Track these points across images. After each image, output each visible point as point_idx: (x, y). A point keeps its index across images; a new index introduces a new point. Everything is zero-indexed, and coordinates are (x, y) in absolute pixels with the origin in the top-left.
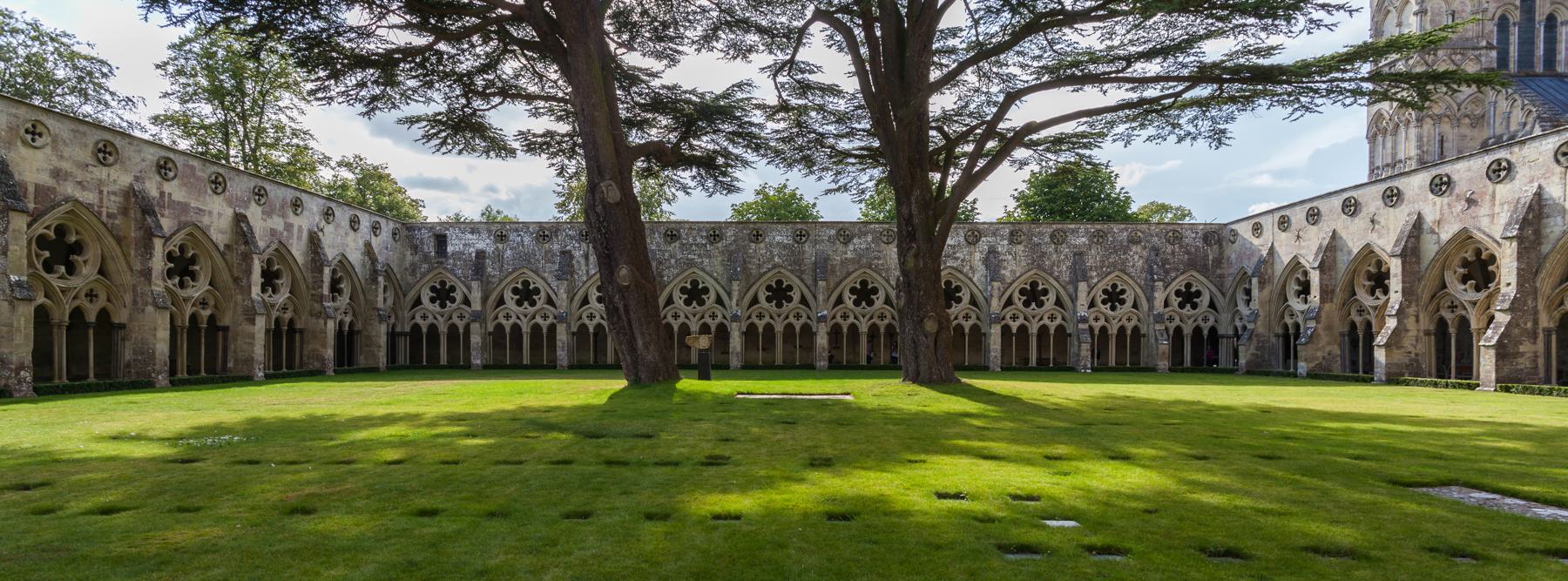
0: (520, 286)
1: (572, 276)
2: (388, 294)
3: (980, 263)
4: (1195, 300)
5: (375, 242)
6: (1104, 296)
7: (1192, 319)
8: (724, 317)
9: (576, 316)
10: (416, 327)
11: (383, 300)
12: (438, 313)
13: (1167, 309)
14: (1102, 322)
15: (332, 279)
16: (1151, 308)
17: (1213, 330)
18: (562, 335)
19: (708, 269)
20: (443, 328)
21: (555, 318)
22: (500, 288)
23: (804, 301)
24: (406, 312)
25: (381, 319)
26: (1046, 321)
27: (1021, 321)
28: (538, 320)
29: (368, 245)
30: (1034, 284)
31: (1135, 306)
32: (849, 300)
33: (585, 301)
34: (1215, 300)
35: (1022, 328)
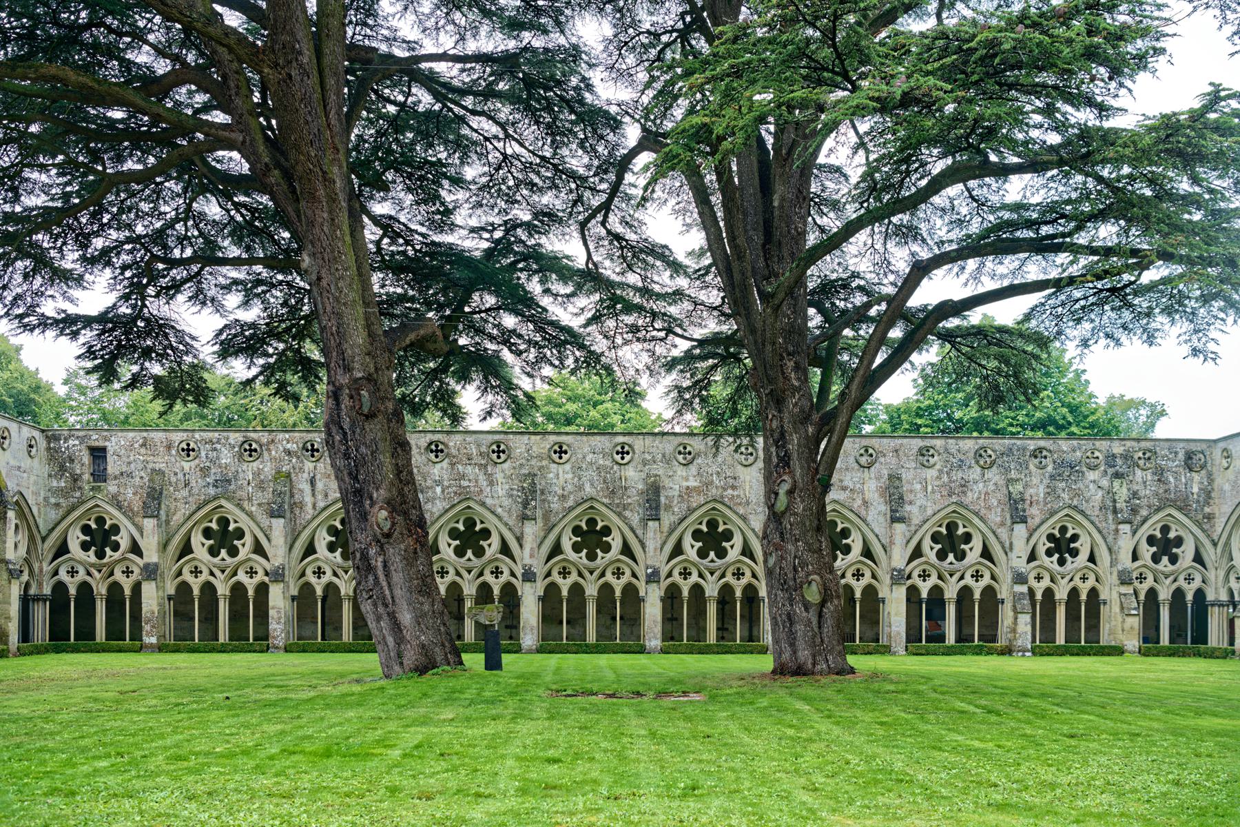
0: (214, 526)
2: (20, 536)
3: (876, 495)
4: (1174, 550)
6: (1049, 545)
7: (1172, 578)
8: (513, 574)
9: (297, 571)
10: (60, 587)
12: (93, 565)
13: (1137, 564)
14: (1046, 582)
17: (1200, 594)
19: (489, 501)
20: (101, 589)
21: (267, 574)
22: (184, 530)
23: (627, 550)
24: (45, 565)
25: (13, 574)
26: (968, 580)
27: (933, 580)
28: (242, 577)
30: (952, 527)
31: (1092, 559)
32: (691, 549)
33: (310, 550)
35: (936, 591)
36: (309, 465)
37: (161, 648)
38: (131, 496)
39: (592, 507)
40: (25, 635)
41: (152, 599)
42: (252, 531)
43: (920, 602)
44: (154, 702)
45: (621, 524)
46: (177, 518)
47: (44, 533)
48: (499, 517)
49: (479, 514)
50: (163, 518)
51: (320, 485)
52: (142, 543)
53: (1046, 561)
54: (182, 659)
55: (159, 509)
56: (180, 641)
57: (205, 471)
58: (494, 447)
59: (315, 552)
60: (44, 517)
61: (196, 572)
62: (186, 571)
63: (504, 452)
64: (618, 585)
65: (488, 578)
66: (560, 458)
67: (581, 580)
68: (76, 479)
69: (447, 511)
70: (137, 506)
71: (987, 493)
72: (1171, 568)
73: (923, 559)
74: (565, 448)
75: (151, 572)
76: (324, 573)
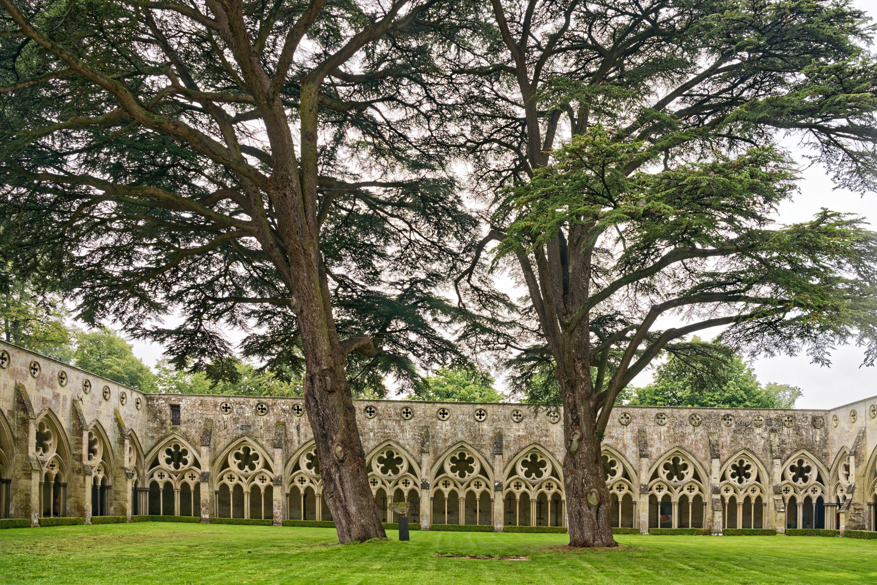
0: (241, 452)
8: (415, 484)
10: (154, 484)
11: (129, 460)
12: (172, 472)
13: (784, 482)
14: (731, 493)
15: (89, 441)
16: (771, 481)
17: (820, 499)
19: (401, 442)
20: (177, 486)
21: (272, 480)
23: (483, 471)
24: (146, 471)
25: (129, 476)
26: (686, 491)
27: (665, 491)
28: (257, 482)
30: (676, 460)
31: (758, 479)
32: (521, 471)
33: (297, 467)
34: (822, 474)
35: (667, 498)
36: (296, 419)
37: (211, 521)
38: (195, 433)
39: (462, 446)
40: (135, 511)
41: (206, 492)
43: (657, 504)
44: (208, 553)
45: (479, 456)
46: (220, 447)
47: (145, 453)
48: (407, 451)
49: (395, 449)
50: (212, 446)
51: (302, 430)
52: (200, 461)
53: (732, 480)
54: (223, 528)
55: (210, 441)
56: (221, 518)
57: (236, 420)
59: (299, 469)
60: (146, 444)
61: (231, 478)
62: (225, 477)
64: (478, 492)
65: (401, 486)
67: (456, 489)
68: (163, 423)
69: (376, 447)
70: (197, 439)
71: (696, 441)
72: (804, 484)
73: (659, 479)
75: (205, 477)
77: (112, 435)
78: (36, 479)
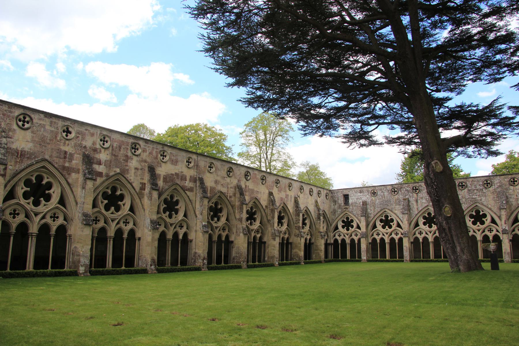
0: (383, 218)
1: (410, 212)
5: (319, 200)
8: (497, 231)
10: (336, 241)
11: (322, 227)
15: (303, 219)
18: (406, 244)
19: (485, 203)
20: (348, 241)
21: (402, 234)
24: (331, 233)
28: (393, 236)
29: (316, 202)
33: (417, 225)
40: (326, 256)
42: (396, 219)
48: (490, 209)
49: (481, 208)
51: (419, 201)
52: (360, 225)
58: (485, 182)
62: (375, 234)
63: (489, 183)
65: (487, 233)
66: (514, 184)
74: (515, 179)
76: (422, 233)
77: (314, 214)
78: (278, 240)
